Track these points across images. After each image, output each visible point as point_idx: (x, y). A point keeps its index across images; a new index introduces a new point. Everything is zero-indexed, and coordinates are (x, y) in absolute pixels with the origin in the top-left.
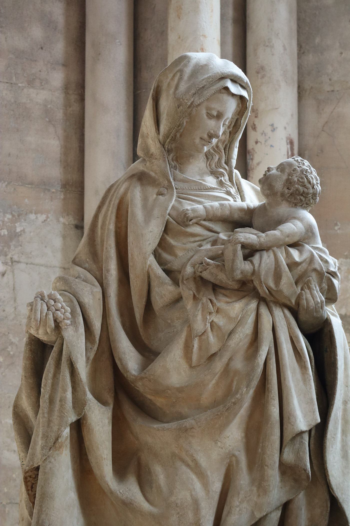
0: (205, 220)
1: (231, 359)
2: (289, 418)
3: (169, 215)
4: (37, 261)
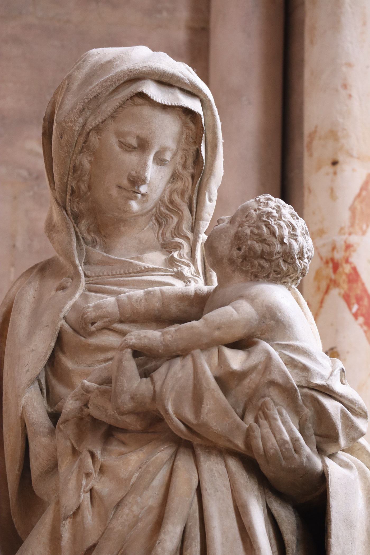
0: (121, 322)
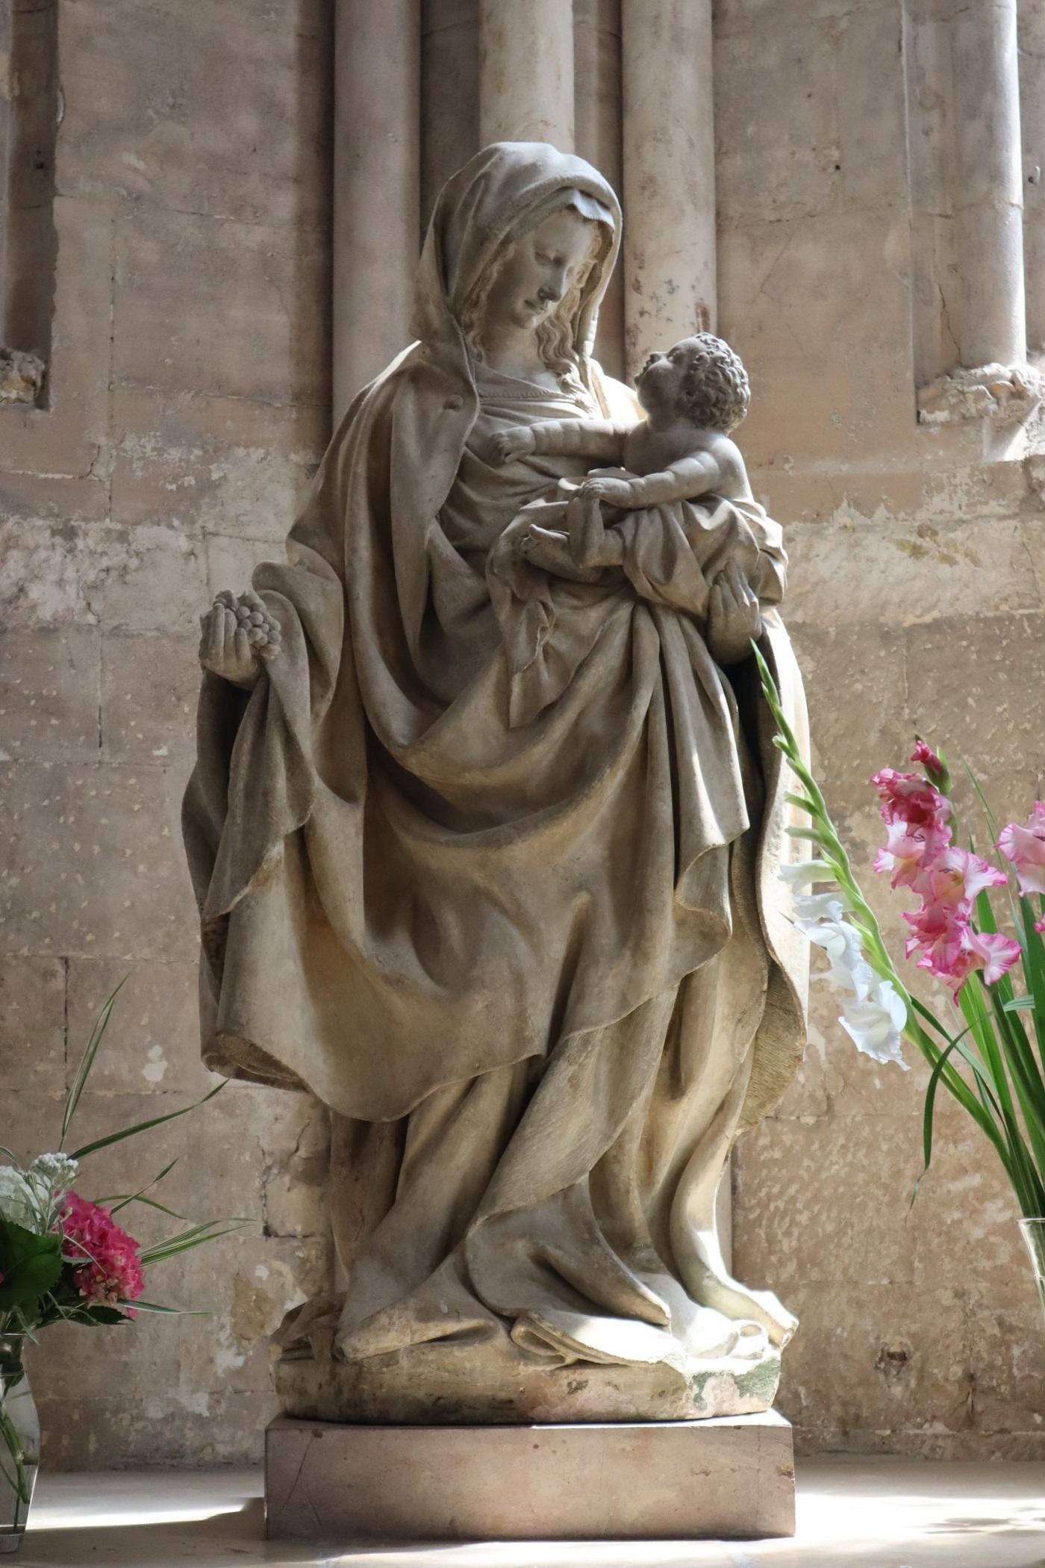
0: (533, 454)
1: (581, 715)
2: (691, 823)
3: (467, 445)
4: (250, 531)
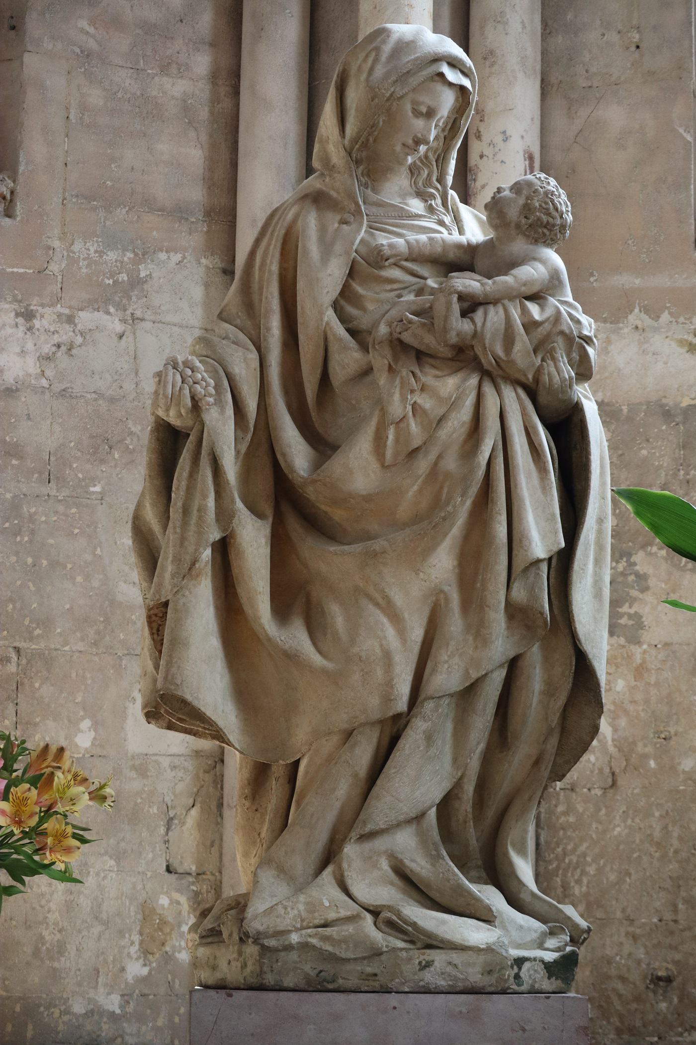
0: (406, 260)
1: (440, 457)
2: (520, 540)
3: (356, 252)
4: (169, 318)
